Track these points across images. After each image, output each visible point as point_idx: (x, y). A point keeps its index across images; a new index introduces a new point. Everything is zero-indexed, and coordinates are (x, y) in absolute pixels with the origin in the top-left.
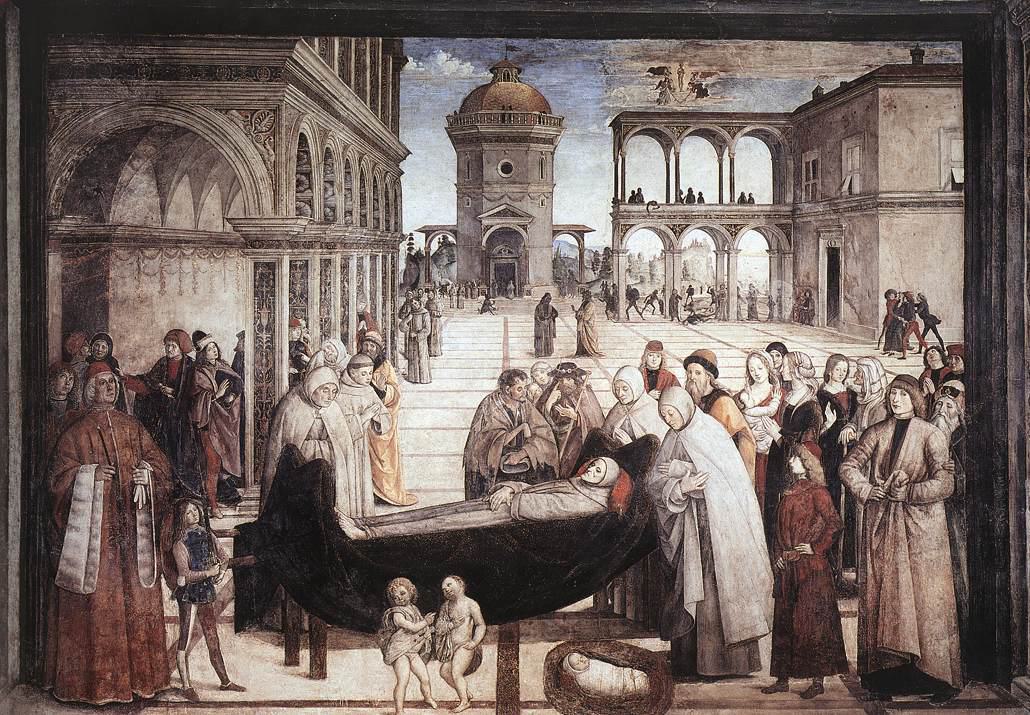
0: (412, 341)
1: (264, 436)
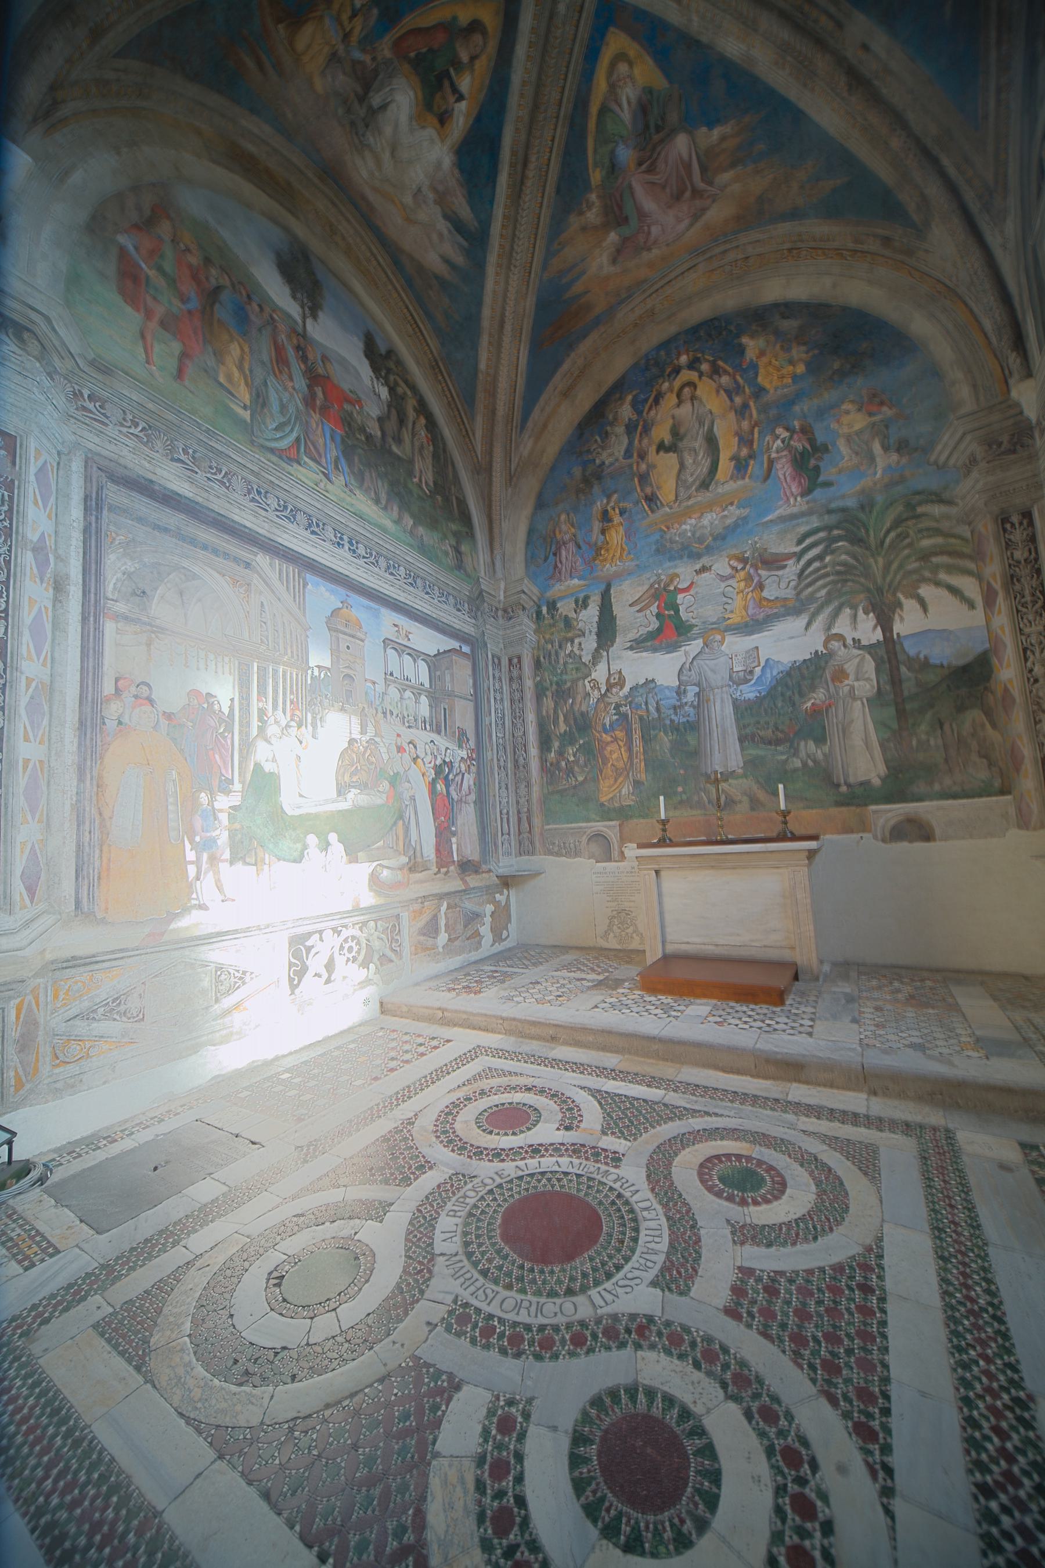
0: (314, 718)
1: (244, 758)
